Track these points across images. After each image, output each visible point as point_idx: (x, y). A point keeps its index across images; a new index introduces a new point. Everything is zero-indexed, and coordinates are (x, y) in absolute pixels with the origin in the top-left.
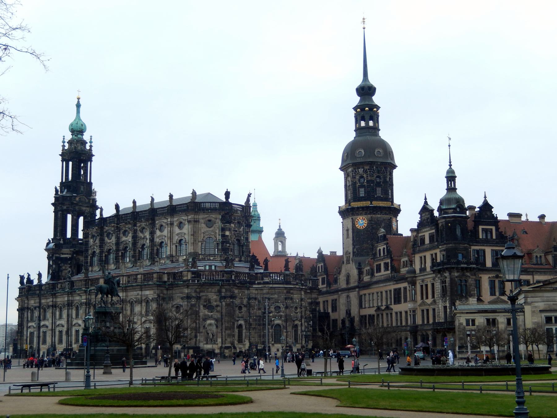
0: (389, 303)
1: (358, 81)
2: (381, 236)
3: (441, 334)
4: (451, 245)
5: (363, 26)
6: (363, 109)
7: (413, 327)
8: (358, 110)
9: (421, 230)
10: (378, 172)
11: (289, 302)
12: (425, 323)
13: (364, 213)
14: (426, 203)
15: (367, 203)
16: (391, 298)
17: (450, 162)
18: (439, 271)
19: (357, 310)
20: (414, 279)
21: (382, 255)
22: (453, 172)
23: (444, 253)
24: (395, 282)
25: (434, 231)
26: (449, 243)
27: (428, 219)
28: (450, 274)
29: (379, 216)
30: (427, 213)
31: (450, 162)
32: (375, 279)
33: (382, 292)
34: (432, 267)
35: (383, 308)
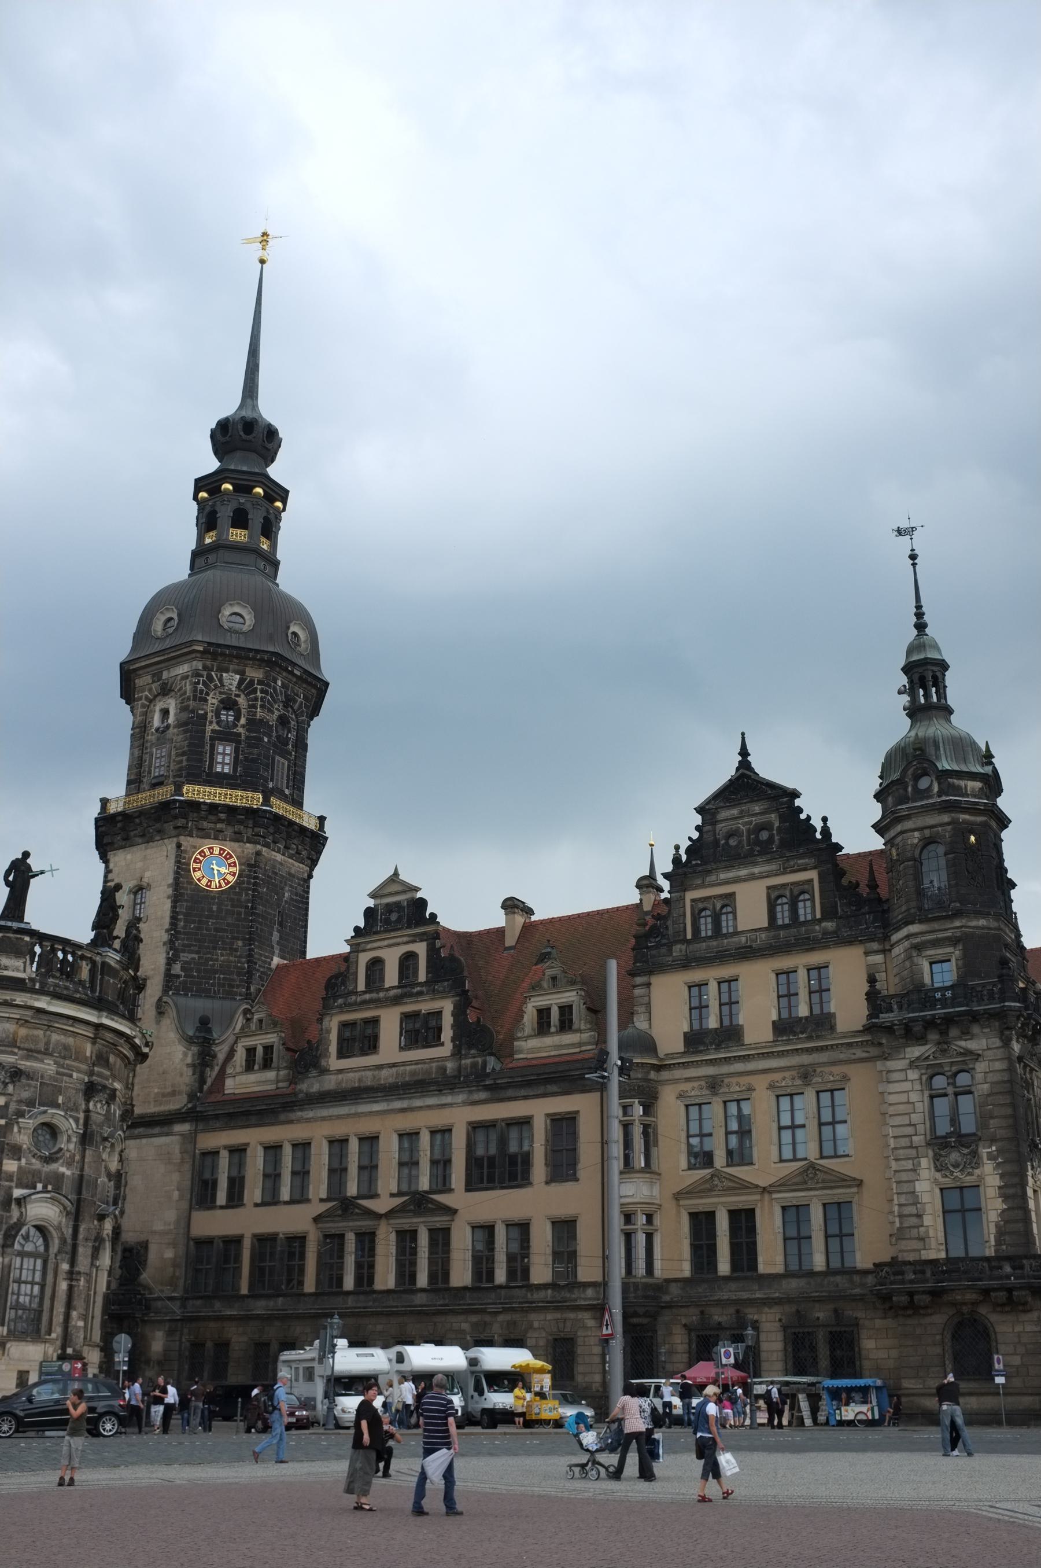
0: (424, 1183)
1: (228, 404)
2: (389, 908)
3: (939, 1319)
4: (982, 922)
5: (260, 254)
6: (243, 488)
7: (646, 1286)
8: (228, 486)
9: (709, 872)
10: (288, 702)
11: (97, 1107)
12: (724, 1267)
13: (229, 831)
14: (745, 764)
15: (254, 800)
16: (442, 1164)
17: (919, 615)
18: (911, 1034)
19: (171, 1215)
20: (653, 1075)
21: (391, 977)
22: (936, 647)
23: (957, 953)
24: (483, 1095)
25: (813, 875)
26: (979, 914)
27: (766, 826)
28: (1006, 1043)
29: (279, 857)
30: (757, 808)
31: (919, 615)
32: (313, 1085)
33: (370, 1141)
34: (783, 1028)
35: (382, 1205)
